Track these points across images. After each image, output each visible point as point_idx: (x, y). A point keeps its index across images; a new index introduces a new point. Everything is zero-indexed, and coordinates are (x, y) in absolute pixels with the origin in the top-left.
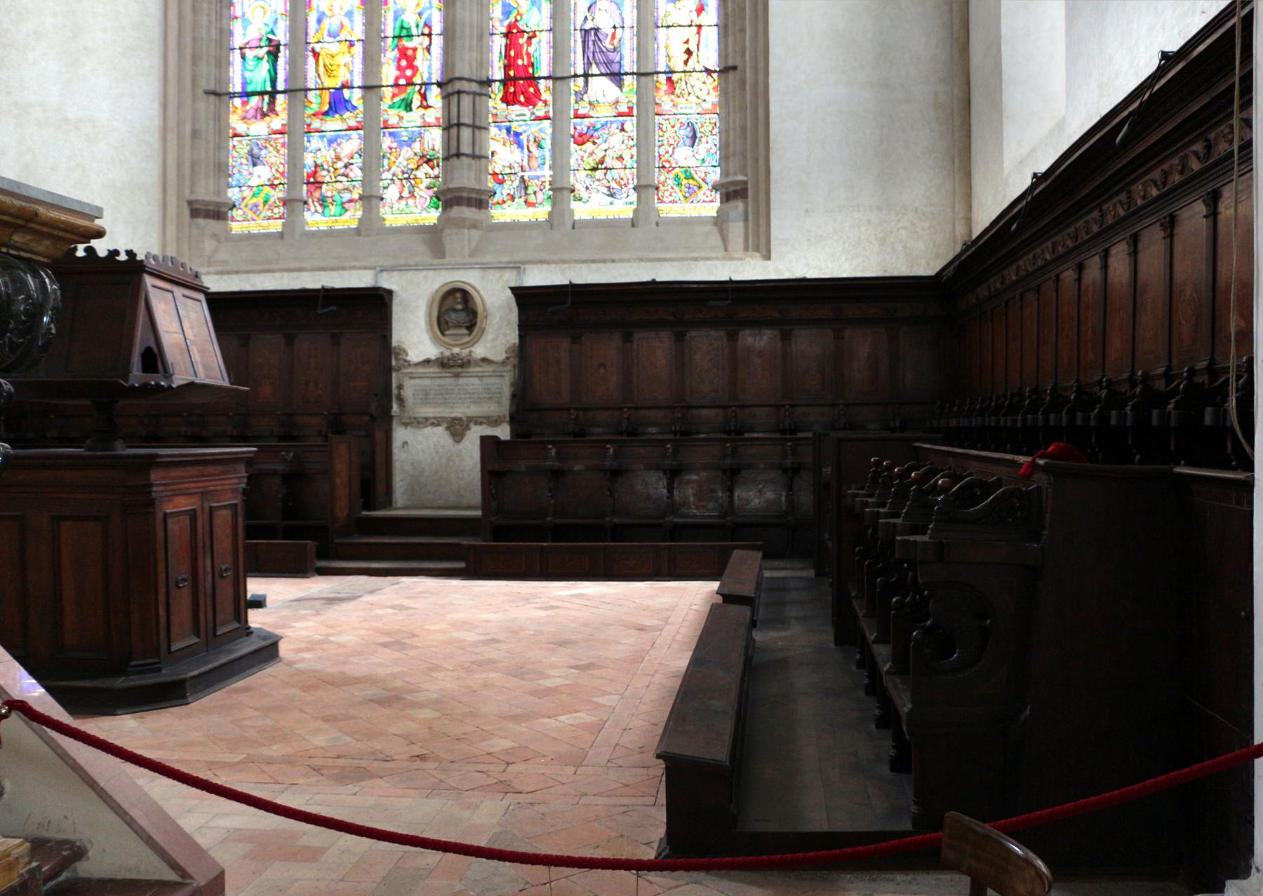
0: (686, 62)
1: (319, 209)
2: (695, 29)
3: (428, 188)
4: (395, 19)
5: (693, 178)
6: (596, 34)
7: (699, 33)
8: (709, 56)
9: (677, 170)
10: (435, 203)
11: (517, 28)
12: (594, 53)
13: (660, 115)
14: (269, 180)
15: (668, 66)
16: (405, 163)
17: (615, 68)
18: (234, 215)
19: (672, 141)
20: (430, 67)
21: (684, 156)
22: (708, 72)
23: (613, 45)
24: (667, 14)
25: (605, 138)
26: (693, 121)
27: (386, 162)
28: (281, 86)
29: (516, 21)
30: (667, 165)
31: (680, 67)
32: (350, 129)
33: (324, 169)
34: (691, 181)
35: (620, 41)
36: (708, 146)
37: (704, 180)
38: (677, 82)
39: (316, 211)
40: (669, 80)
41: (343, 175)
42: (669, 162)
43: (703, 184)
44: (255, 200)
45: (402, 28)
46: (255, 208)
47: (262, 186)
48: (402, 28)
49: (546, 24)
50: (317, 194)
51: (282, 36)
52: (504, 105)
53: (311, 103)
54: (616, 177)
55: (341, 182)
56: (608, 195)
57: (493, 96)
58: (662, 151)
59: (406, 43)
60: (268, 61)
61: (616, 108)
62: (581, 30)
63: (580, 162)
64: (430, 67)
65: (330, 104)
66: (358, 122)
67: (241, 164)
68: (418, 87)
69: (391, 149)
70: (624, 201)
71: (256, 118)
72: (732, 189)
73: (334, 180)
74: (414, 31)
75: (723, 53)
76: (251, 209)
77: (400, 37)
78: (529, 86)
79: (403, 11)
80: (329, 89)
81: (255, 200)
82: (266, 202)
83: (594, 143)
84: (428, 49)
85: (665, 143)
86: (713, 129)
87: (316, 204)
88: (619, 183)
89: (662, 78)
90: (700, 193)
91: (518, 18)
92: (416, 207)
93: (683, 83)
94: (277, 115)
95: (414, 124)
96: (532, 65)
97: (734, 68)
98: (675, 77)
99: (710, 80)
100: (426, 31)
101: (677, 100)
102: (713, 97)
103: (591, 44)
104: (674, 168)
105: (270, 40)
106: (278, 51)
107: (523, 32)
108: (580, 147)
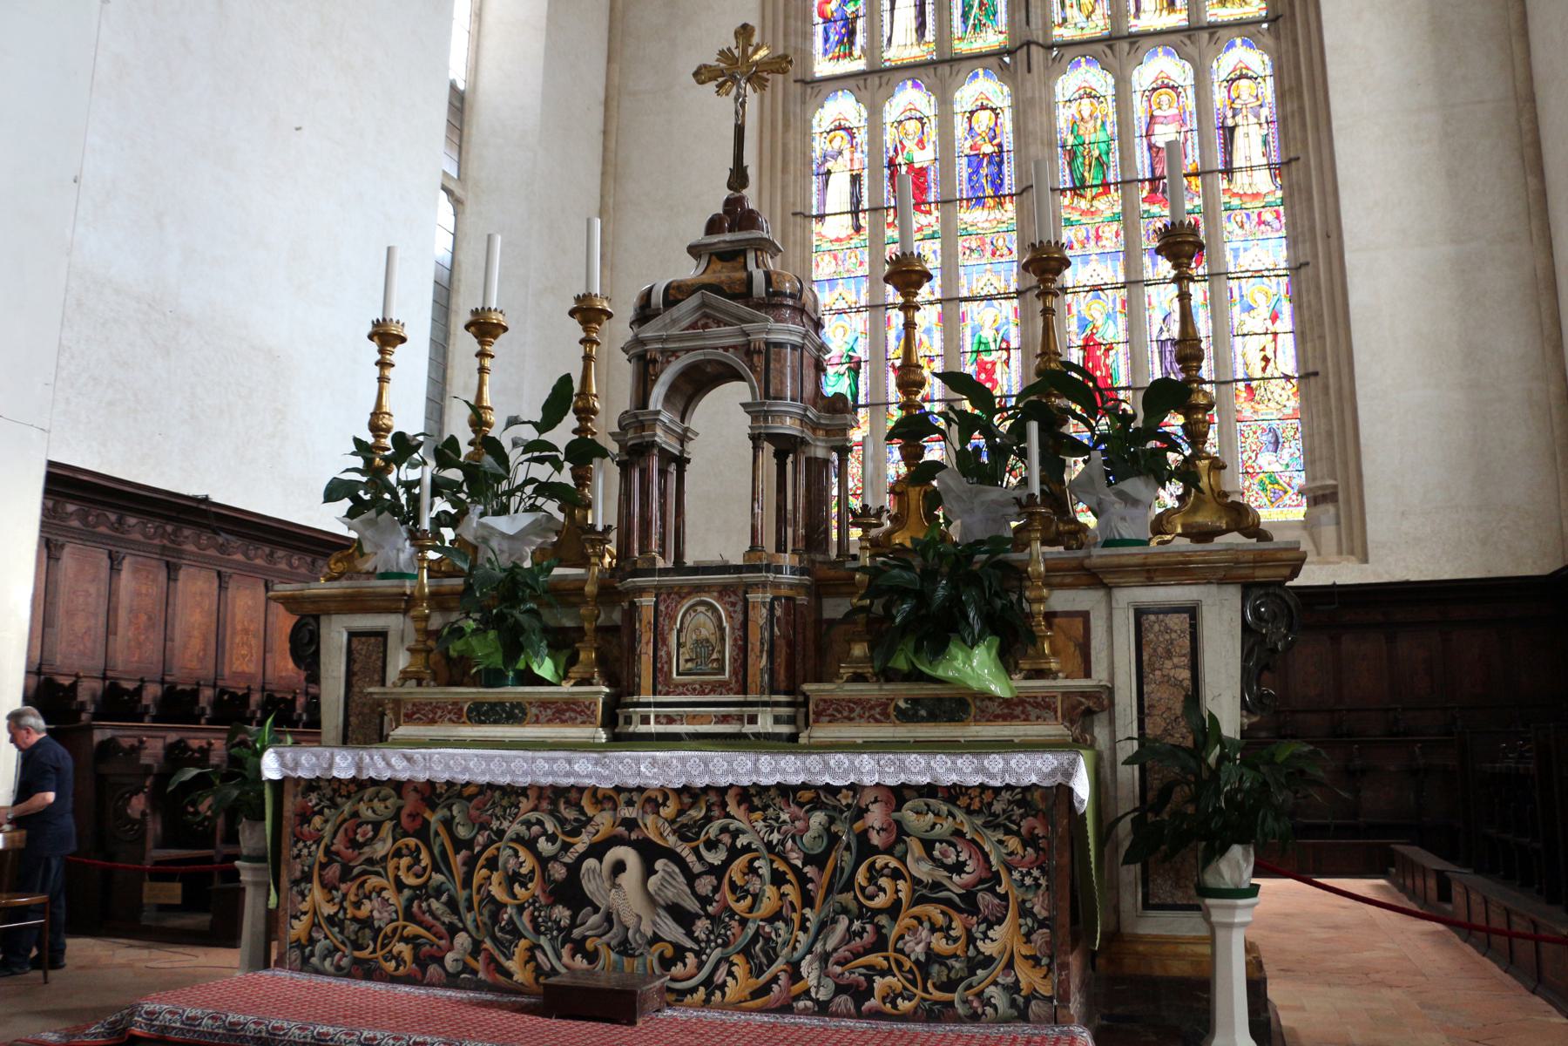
0: (1264, 369)
2: (1270, 337)
4: (973, 335)
7: (1275, 340)
8: (1287, 362)
9: (1261, 476)
11: (1093, 340)
15: (1246, 374)
19: (1254, 447)
20: (1009, 380)
21: (1267, 461)
22: (1287, 378)
24: (1242, 323)
26: (1275, 426)
28: (862, 400)
29: (1093, 334)
30: (1251, 470)
31: (1258, 374)
34: (1276, 486)
36: (1291, 451)
37: (1289, 485)
40: (1248, 387)
43: (1289, 489)
48: (980, 343)
49: (1122, 337)
51: (862, 352)
58: (1245, 457)
59: (985, 357)
64: (1009, 380)
72: (1320, 492)
74: (992, 346)
75: (1301, 358)
77: (978, 352)
79: (981, 328)
84: (1007, 362)
89: (1241, 385)
90: (1286, 498)
97: (1316, 374)
98: (1254, 384)
99: (1290, 386)
100: (1004, 345)
101: (1257, 406)
102: (1294, 403)
103: (1168, 354)
105: (851, 357)
106: (860, 367)
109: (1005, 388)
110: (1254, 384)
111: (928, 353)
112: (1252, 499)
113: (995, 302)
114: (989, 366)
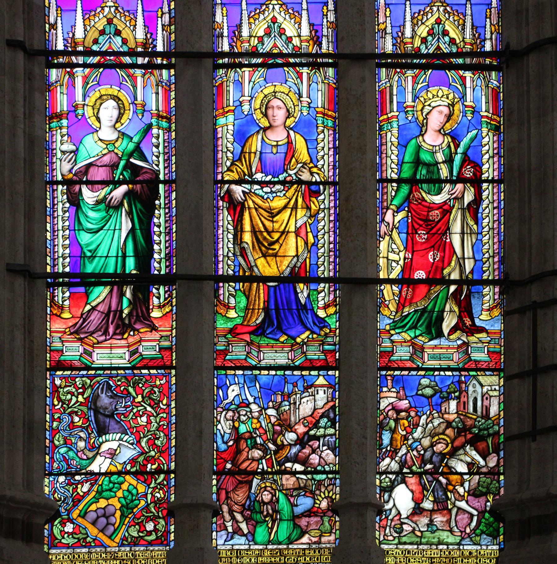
1: (243, 526)
3: (475, 493)
4: (403, 145)
10: (488, 525)
14: (133, 461)
16: (426, 442)
18: (56, 531)
27: (386, 438)
32: (310, 365)
33: (255, 446)
39: (237, 531)
41: (296, 459)
44: (102, 503)
45: (417, 162)
46: (103, 521)
47: (119, 473)
48: (417, 162)
50: (240, 496)
53: (228, 307)
55: (294, 473)
60: (130, 213)
65: (266, 310)
66: (324, 352)
67: (72, 425)
68: (453, 288)
69: (398, 411)
71: (106, 333)
73: (276, 468)
74: (444, 172)
76: (94, 523)
77: (413, 182)
80: (265, 279)
81: (102, 503)
82: (126, 509)
87: (239, 517)
92: (451, 531)
94: (154, 328)
95: (444, 364)
105: (135, 170)
106: (156, 196)
109: (469, 265)
111: (305, 176)
113: (451, 74)
114: (436, 214)
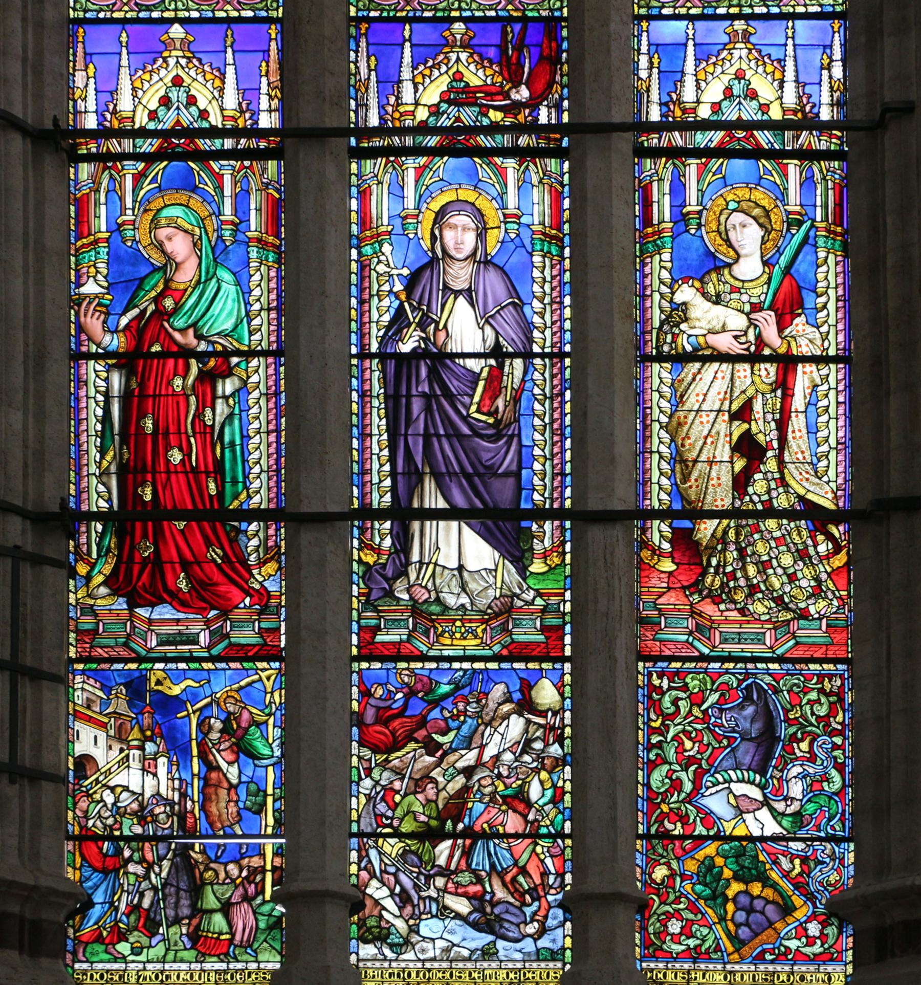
0: (741, 482)
5: (765, 881)
6: (434, 376)
7: (784, 384)
9: (710, 849)
12: (427, 437)
13: (655, 659)
15: (677, 492)
17: (503, 492)
23: (493, 413)
25: (465, 729)
34: (756, 889)
35: (516, 399)
37: (800, 886)
38: (711, 550)
42: (684, 819)
43: (798, 901)
52: (121, 604)
54: (505, 860)
56: (475, 926)
57: (82, 569)
58: (658, 777)
61: (505, 630)
62: (382, 356)
63: (382, 808)
70: (528, 945)
78: (208, 544)
83: (431, 747)
85: (671, 754)
86: (832, 713)
88: (512, 886)
90: (787, 928)
91: (169, 303)
93: (732, 554)
96: (219, 465)
98: (707, 529)
101: (709, 609)
103: (417, 406)
104: (701, 840)
107: (187, 353)
108: (381, 758)
110: (707, 529)
112: (675, 927)
